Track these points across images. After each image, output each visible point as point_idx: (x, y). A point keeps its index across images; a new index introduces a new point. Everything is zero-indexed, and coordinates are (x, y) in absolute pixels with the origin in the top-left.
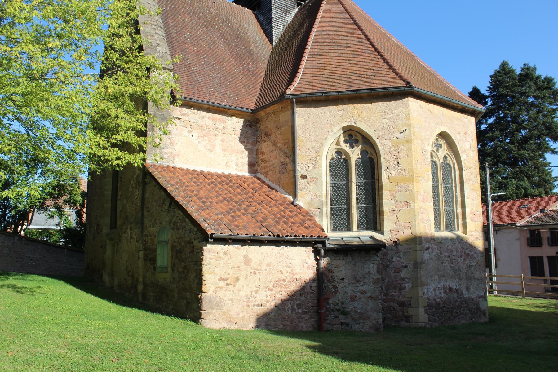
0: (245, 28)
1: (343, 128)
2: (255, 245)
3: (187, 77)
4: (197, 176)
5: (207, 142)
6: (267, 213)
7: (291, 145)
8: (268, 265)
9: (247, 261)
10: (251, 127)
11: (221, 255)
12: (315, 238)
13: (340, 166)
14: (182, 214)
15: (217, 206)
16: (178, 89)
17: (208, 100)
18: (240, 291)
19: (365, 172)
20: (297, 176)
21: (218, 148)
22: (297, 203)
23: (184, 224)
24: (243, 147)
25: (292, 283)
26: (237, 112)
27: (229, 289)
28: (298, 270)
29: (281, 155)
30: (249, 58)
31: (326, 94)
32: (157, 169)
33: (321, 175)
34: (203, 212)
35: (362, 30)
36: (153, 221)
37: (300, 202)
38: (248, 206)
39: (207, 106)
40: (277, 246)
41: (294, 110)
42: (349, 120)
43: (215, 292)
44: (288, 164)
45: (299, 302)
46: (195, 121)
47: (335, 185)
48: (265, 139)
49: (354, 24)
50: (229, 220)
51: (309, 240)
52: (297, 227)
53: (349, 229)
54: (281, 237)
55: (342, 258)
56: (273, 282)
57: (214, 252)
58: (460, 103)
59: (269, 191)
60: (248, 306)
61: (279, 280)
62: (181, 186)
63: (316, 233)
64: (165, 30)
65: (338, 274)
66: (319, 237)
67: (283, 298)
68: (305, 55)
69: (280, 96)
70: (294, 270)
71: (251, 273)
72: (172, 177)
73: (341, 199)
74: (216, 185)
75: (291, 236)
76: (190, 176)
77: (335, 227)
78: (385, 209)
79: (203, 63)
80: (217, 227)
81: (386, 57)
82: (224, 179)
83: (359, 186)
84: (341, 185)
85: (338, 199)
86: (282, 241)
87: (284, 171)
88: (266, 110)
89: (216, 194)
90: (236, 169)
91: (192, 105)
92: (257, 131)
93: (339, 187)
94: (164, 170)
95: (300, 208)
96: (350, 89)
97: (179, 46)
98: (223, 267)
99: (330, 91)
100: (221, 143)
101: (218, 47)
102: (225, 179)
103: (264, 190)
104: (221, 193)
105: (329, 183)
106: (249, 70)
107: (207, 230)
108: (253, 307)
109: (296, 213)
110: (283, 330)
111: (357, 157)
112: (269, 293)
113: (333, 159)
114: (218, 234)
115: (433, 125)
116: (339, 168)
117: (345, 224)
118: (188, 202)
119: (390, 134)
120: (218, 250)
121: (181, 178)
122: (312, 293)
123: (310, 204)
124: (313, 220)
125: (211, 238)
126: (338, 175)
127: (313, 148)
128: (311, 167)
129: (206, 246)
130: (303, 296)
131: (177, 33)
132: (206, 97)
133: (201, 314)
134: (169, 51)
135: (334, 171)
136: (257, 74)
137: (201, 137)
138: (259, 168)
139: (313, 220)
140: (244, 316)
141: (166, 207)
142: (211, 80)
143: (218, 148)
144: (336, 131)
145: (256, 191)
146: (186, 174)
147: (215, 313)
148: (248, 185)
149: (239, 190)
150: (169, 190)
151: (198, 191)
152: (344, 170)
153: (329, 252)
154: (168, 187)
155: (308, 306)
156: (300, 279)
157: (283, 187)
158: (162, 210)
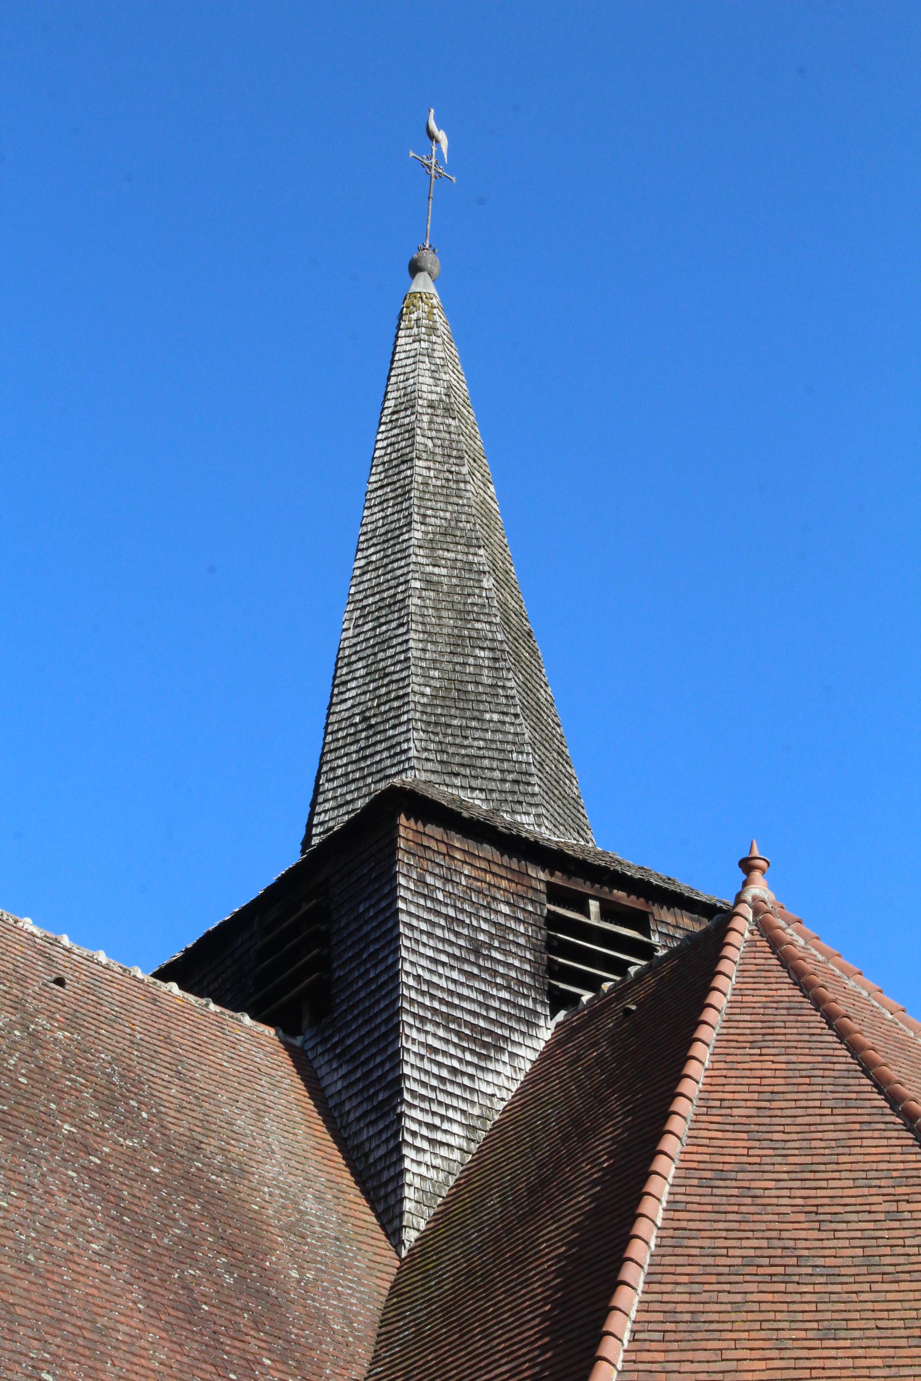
0: (237, 1136)
30: (257, 1325)
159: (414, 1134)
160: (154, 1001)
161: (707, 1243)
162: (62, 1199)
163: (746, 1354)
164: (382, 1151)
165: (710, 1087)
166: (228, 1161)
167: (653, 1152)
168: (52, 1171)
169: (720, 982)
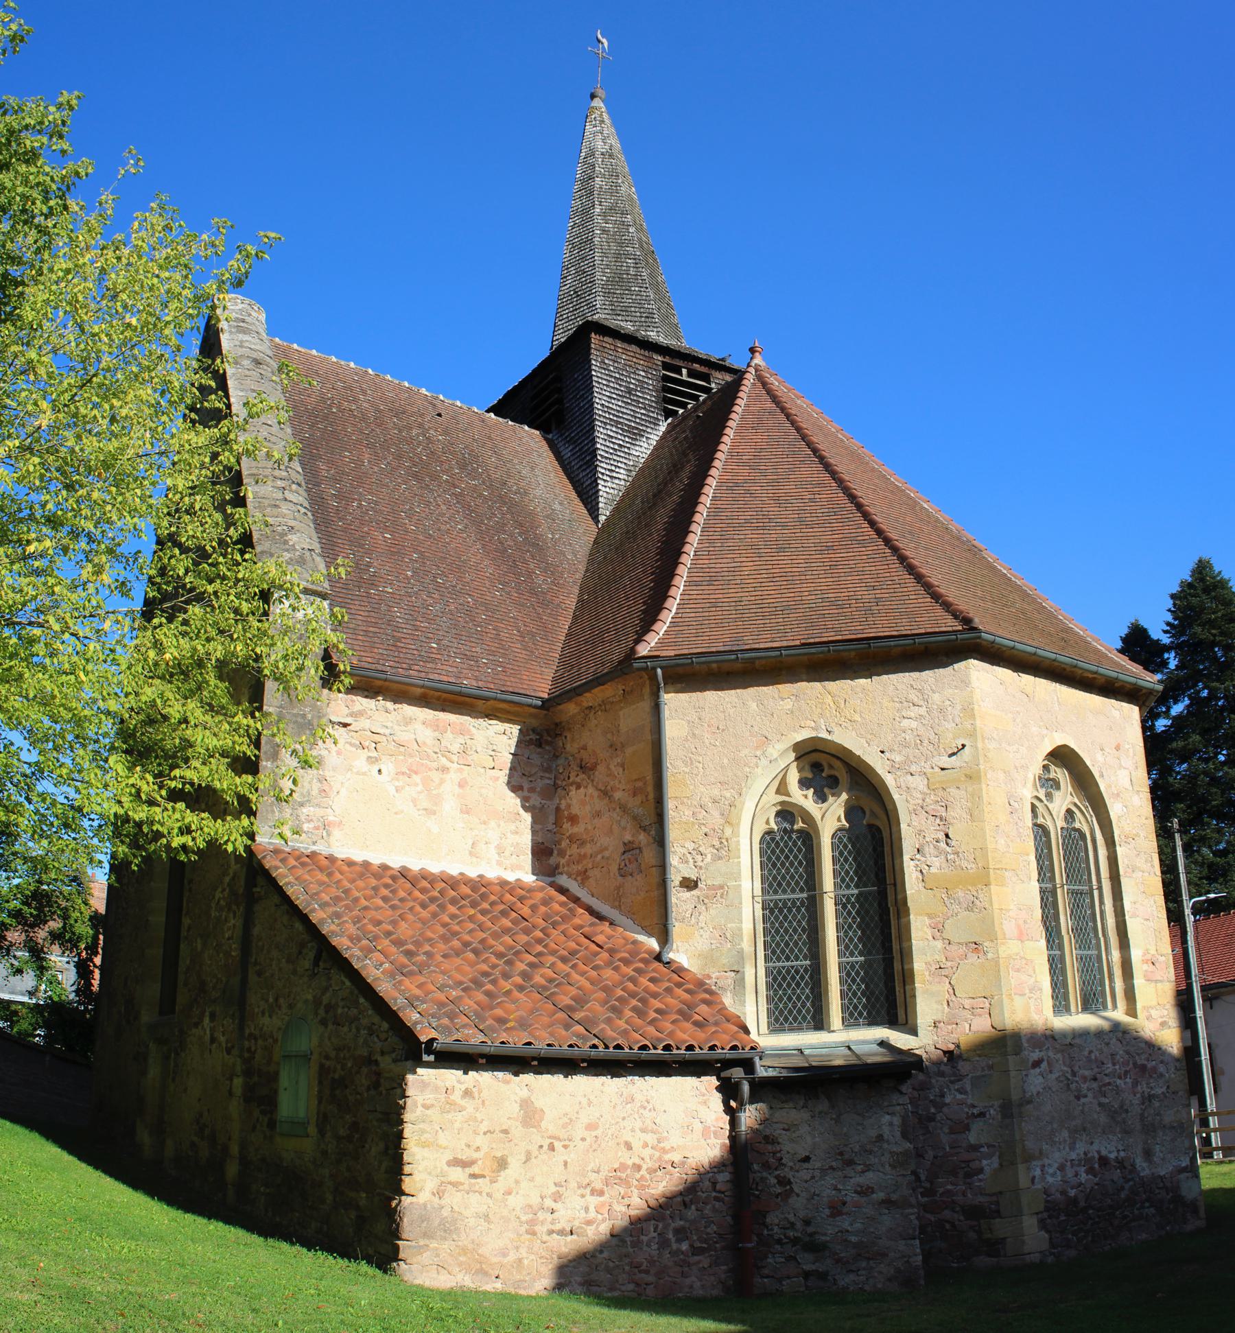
0: (522, 478)
1: (797, 747)
2: (552, 1074)
3: (366, 614)
4: (390, 881)
5: (420, 788)
6: (587, 984)
7: (651, 796)
8: (591, 1127)
9: (530, 1115)
10: (540, 745)
11: (456, 1096)
12: (724, 1053)
13: (791, 851)
14: (348, 983)
15: (446, 965)
17: (423, 675)
18: (510, 1193)
19: (859, 866)
20: (669, 882)
21: (450, 806)
23: (355, 1011)
24: (518, 801)
25: (659, 1173)
27: (477, 1188)
28: (675, 1140)
29: (623, 823)
30: (533, 557)
31: (747, 655)
32: (283, 861)
33: (737, 877)
34: (407, 981)
35: (840, 482)
36: (271, 1000)
37: (680, 954)
38: (531, 965)
39: (419, 691)
40: (615, 1075)
41: (658, 697)
42: (813, 724)
43: (439, 1193)
44: (644, 850)
45: (682, 1223)
46: (387, 732)
47: (776, 904)
48: (578, 779)
49: (820, 467)
51: (708, 1057)
52: (673, 1022)
53: (819, 1022)
55: (801, 1103)
56: (603, 1175)
57: (436, 1089)
58: (1101, 671)
59: (592, 925)
60: (534, 1234)
61: (623, 1167)
63: (726, 1037)
65: (791, 1147)
66: (734, 1048)
67: (634, 1212)
68: (687, 548)
69: (620, 663)
70: (666, 1139)
71: (541, 1147)
72: (324, 883)
73: (796, 944)
74: (442, 907)
75: (655, 1048)
76: (373, 882)
77: (780, 1020)
78: (919, 965)
79: (409, 573)
80: (446, 1021)
81: (908, 553)
82: (466, 890)
83: (844, 907)
84: (794, 903)
85: (787, 944)
86: (630, 1061)
87: (632, 867)
89: (442, 931)
90: (499, 863)
91: (380, 687)
92: (556, 757)
93: (790, 910)
94: (303, 865)
95: (679, 971)
96: (812, 641)
98: (460, 1130)
99: (757, 646)
100: (457, 790)
101: (448, 531)
102: (469, 891)
103: (577, 921)
104: (457, 928)
105: (759, 899)
106: (533, 592)
108: (545, 1238)
109: (668, 984)
110: (635, 1295)
111: (836, 825)
112: (593, 1201)
113: (769, 832)
114: (449, 1040)
115: (1034, 729)
116: (787, 857)
117: (808, 1011)
118: (367, 951)
121: (348, 885)
122: (716, 1199)
123: (708, 957)
124: (716, 1003)
126: (784, 878)
127: (715, 802)
128: (709, 856)
130: (693, 1207)
135: (774, 865)
136: (557, 601)
137: (403, 773)
138: (563, 861)
139: (716, 1003)
140: (520, 1260)
141: (307, 964)
143: (450, 806)
144: (775, 755)
145: (554, 925)
146: (361, 876)
148: (534, 908)
149: (506, 922)
150: (315, 918)
151: (394, 923)
152: (800, 863)
153: (764, 1089)
154: (314, 910)
155: (708, 1234)
156: (683, 1163)
157: (630, 914)
158: (295, 972)
159: (603, 474)
160: (483, 421)
161: (729, 514)
162: (444, 507)
164: (589, 482)
165: (733, 446)
166: (518, 489)
167: (706, 476)
168: (439, 496)
169: (738, 401)
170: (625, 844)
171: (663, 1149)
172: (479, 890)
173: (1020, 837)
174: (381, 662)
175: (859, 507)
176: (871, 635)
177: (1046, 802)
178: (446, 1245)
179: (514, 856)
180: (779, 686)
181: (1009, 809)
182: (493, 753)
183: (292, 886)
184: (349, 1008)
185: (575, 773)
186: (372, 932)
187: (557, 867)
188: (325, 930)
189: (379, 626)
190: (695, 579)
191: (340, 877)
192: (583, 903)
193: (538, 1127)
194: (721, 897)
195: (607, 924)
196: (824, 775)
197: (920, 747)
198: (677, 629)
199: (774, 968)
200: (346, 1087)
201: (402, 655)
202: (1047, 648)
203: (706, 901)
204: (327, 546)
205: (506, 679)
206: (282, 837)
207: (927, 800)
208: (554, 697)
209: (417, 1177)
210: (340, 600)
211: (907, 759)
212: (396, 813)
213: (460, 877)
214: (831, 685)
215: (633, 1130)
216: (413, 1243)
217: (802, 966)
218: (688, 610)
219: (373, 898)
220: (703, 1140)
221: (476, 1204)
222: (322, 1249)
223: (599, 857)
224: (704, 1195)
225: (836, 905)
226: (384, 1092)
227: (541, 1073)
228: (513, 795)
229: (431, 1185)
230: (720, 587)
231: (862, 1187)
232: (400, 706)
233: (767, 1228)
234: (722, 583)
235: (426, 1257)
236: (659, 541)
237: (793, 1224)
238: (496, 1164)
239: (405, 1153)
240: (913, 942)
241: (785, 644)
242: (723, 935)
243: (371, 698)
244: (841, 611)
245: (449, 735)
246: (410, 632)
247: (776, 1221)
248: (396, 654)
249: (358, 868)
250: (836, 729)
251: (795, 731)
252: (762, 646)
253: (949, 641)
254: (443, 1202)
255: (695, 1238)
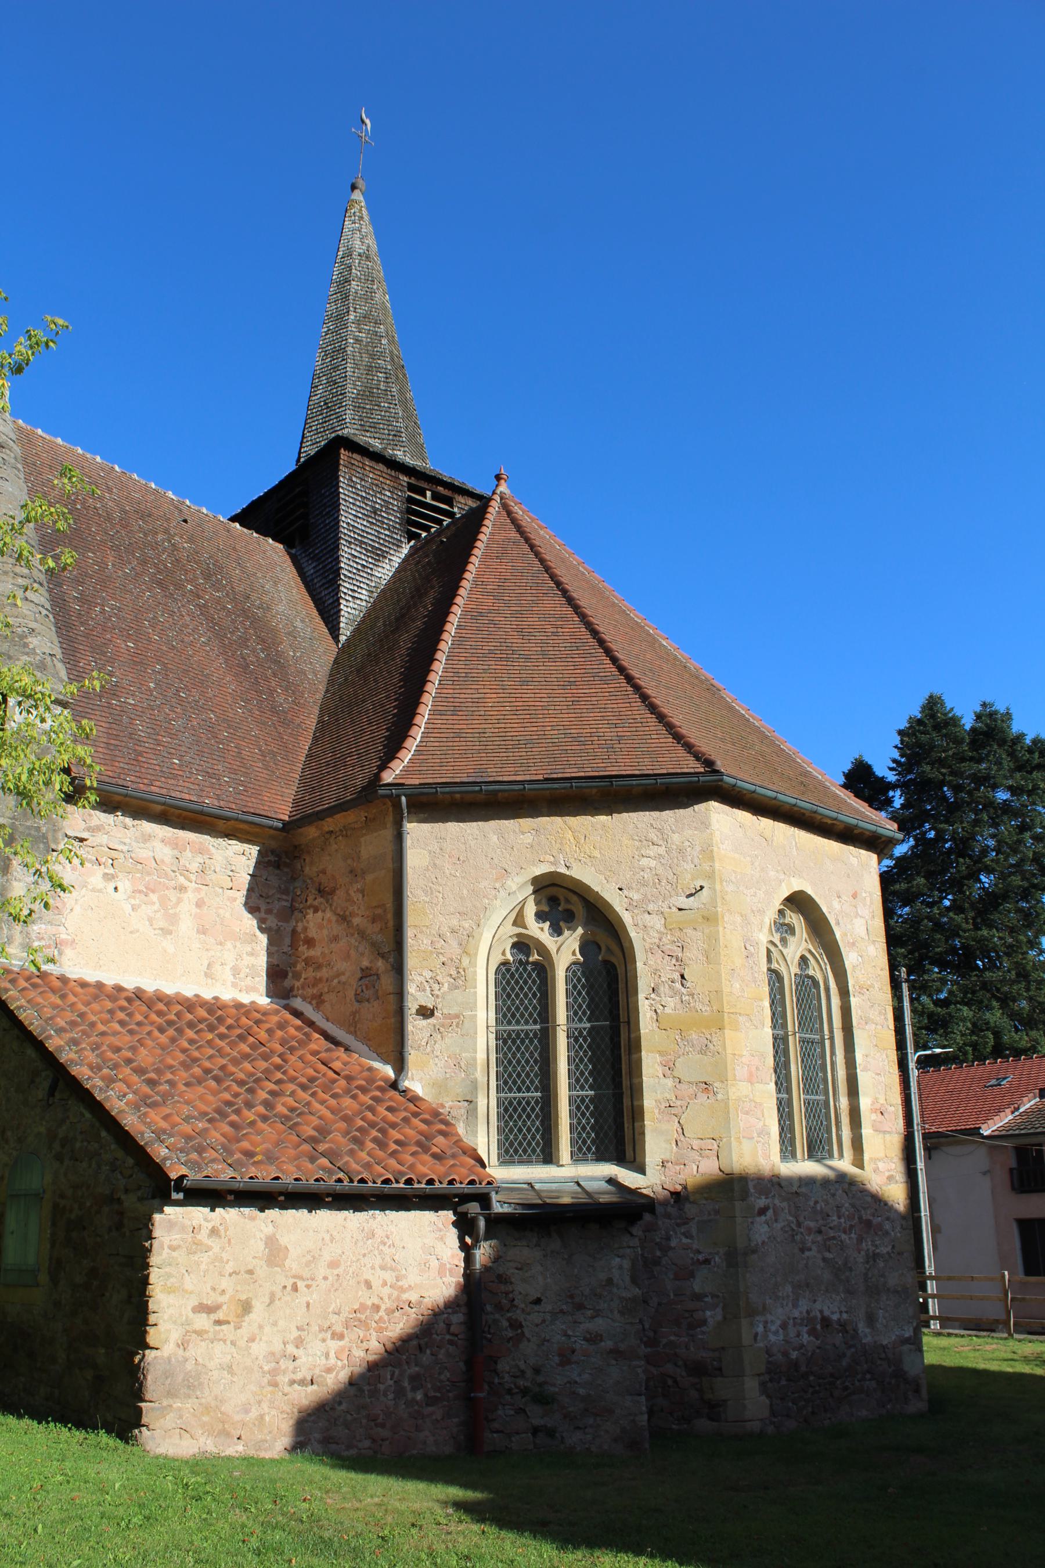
0: (266, 593)
2: (297, 1209)
3: (107, 725)
4: (125, 1004)
5: (157, 906)
6: (328, 1114)
7: (391, 924)
8: (333, 1264)
9: (275, 1253)
10: (278, 867)
11: (203, 1236)
12: (461, 1187)
13: (525, 982)
14: (88, 1115)
16: (89, 761)
17: (164, 792)
18: (252, 1340)
19: (592, 1000)
21: (186, 926)
22: (406, 1084)
23: (96, 1145)
24: (255, 922)
25: (397, 1314)
26: (242, 826)
27: (221, 1336)
28: (413, 1278)
29: (361, 949)
30: (275, 675)
31: (491, 788)
32: (13, 981)
33: (473, 1007)
35: (583, 617)
37: (415, 1083)
38: (272, 1093)
40: (357, 1209)
43: (183, 1345)
45: (417, 1369)
46: (125, 848)
48: (316, 903)
49: (563, 601)
50: (224, 1135)
52: (413, 1154)
53: (549, 1157)
54: (370, 1184)
56: (345, 1314)
57: (183, 1228)
59: (328, 1050)
60: (275, 1385)
61: (363, 1307)
62: (84, 1032)
63: (464, 1171)
64: (50, 591)
66: (472, 1182)
67: (371, 1358)
69: (364, 788)
70: (405, 1277)
71: (285, 1287)
72: (58, 1006)
73: (528, 1075)
74: (181, 1031)
75: (397, 1182)
76: (109, 1005)
77: (510, 1154)
78: (649, 1102)
80: (194, 1156)
81: (649, 692)
82: (202, 1013)
83: (576, 1040)
84: (527, 1034)
85: (519, 1075)
86: (373, 1196)
87: (368, 993)
88: (324, 823)
89: (182, 1057)
90: (234, 985)
91: (119, 802)
92: (294, 879)
93: (523, 1042)
94: (35, 986)
95: (415, 1099)
96: (555, 776)
97: (87, 636)
98: (206, 1271)
99: (500, 779)
100: (195, 910)
102: (205, 1014)
103: (313, 1046)
104: (196, 1054)
105: (493, 1030)
106: (274, 710)
107: (168, 1163)
108: (287, 1389)
109: (404, 1114)
111: (571, 959)
112: (334, 1345)
113: (505, 963)
114: (199, 1176)
115: (772, 873)
116: (521, 988)
117: (538, 1144)
118: (110, 1081)
119: (661, 898)
120: (195, 1223)
121: (83, 1009)
122: (451, 1342)
123: (441, 1086)
125: (178, 1189)
126: (518, 1009)
128: (446, 985)
129: (162, 1212)
130: (428, 1352)
131: (82, 599)
132: (158, 784)
133: (139, 1412)
134: (60, 651)
135: (509, 996)
136: (298, 721)
137: (140, 892)
138: (297, 984)
140: (262, 1417)
141: (41, 1093)
142: (173, 736)
143: (186, 926)
144: (514, 888)
145: (292, 1049)
146: (96, 997)
147: (179, 1409)
148: (270, 1032)
149: (244, 1048)
150: (51, 1045)
151: (133, 1049)
152: (534, 995)
153: (498, 1224)
154: (50, 1037)
155: (441, 1381)
156: (420, 1303)
157: (366, 1040)
159: (345, 594)
160: (228, 531)
161: (473, 643)
162: (188, 618)
163: (488, 691)
164: (330, 601)
168: (183, 606)
169: (484, 529)
170: (362, 970)
171: (401, 1287)
172: (215, 1012)
173: (755, 982)
174: (122, 776)
175: (601, 642)
176: (614, 773)
177: (780, 947)
178: (189, 1405)
179: (249, 978)
180: (520, 820)
181: (745, 953)
182: (231, 874)
183: (25, 1011)
184: (89, 1142)
185: (314, 896)
186: (111, 1060)
187: (292, 989)
188: (63, 1058)
189: (119, 738)
190: (440, 708)
191: (75, 999)
192: (318, 1027)
193: (281, 1265)
194: (457, 1026)
195: (342, 1049)
196: (560, 908)
197: (658, 886)
198: (421, 757)
199: (506, 1099)
200: (84, 1228)
201: (143, 770)
202: (787, 793)
203: (442, 1029)
204: (68, 652)
205: (248, 799)
206: (35, 965)
207: (664, 939)
208: (298, 820)
209: (162, 1327)
210: (80, 709)
211: (645, 899)
212: (131, 932)
213: (196, 999)
214: (572, 821)
215: (373, 1268)
216: (157, 1405)
217: (533, 1098)
218: (432, 739)
219: (110, 1022)
220: (438, 1278)
221: (221, 1353)
222: (55, 1421)
223: (336, 981)
224: (439, 1338)
225: (568, 1037)
226: (128, 1234)
227: (287, 1209)
228: (250, 916)
229: (175, 1335)
230: (464, 717)
231: (591, 1334)
232: (139, 822)
233: (498, 1375)
234: (466, 713)
235: (169, 1421)
236: (402, 667)
237: (523, 1372)
238: (241, 1308)
239: (151, 1301)
240: (644, 1078)
241: (528, 778)
242: (456, 1065)
243: (110, 813)
244: (583, 747)
245: (188, 854)
246: (152, 746)
247: (507, 1368)
248: (138, 768)
249: (92, 990)
250: (574, 865)
251: (534, 865)
252: (506, 779)
253: (690, 782)
254: (187, 1354)
255: (429, 1386)
